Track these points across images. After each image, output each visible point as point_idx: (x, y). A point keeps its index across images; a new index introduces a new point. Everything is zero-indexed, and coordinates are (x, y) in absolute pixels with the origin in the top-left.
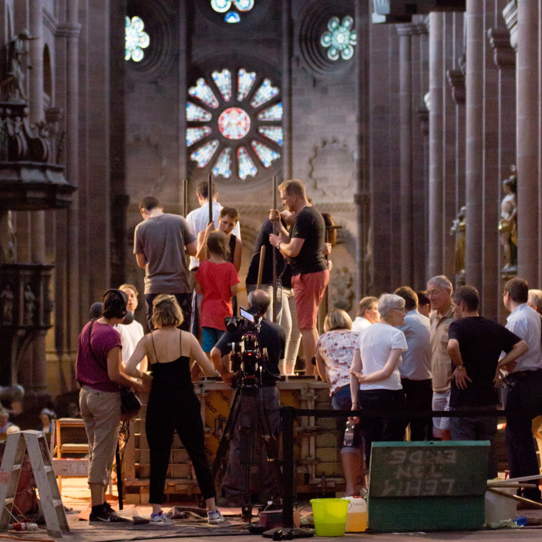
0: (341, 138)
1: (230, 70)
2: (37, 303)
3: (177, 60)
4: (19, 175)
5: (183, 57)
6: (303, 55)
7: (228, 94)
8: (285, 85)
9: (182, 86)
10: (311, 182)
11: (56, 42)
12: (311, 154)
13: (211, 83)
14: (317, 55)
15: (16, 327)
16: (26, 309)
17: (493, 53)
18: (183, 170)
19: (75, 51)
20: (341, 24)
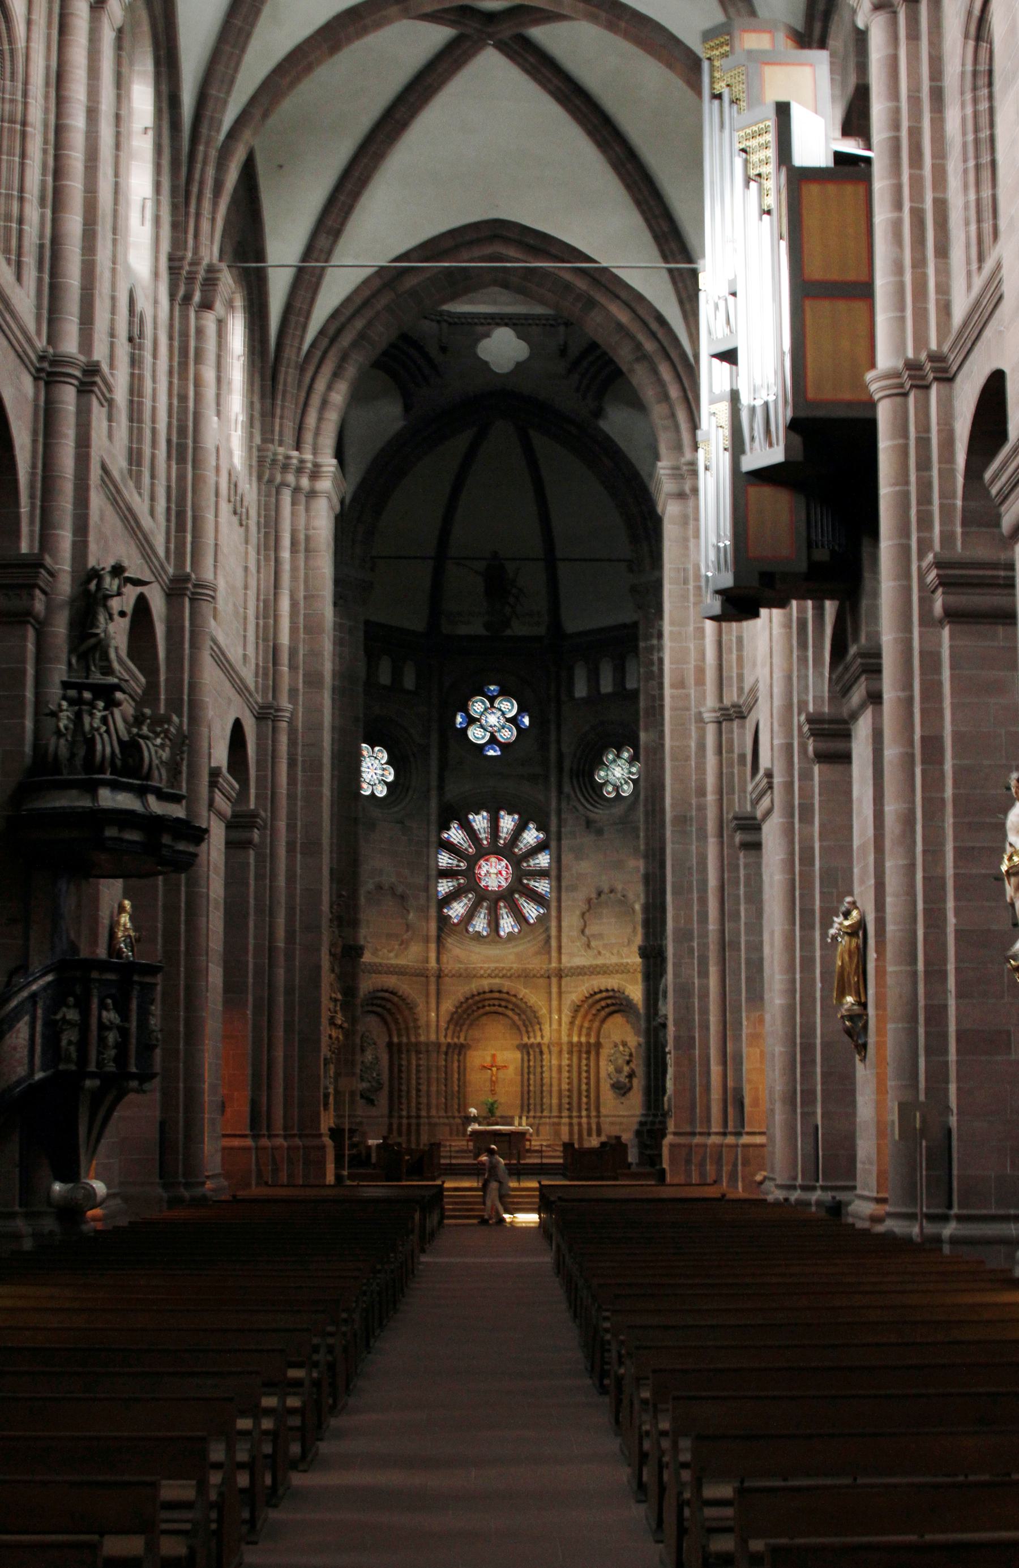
0: (619, 887)
1: (488, 812)
2: (124, 1032)
4: (95, 797)
5: (434, 793)
6: (575, 792)
7: (486, 838)
8: (553, 828)
9: (434, 828)
10: (584, 939)
11: (258, 726)
13: (467, 827)
14: (591, 792)
15: (82, 1074)
16: (102, 1040)
17: (932, 602)
18: (433, 926)
19: (284, 739)
20: (618, 756)
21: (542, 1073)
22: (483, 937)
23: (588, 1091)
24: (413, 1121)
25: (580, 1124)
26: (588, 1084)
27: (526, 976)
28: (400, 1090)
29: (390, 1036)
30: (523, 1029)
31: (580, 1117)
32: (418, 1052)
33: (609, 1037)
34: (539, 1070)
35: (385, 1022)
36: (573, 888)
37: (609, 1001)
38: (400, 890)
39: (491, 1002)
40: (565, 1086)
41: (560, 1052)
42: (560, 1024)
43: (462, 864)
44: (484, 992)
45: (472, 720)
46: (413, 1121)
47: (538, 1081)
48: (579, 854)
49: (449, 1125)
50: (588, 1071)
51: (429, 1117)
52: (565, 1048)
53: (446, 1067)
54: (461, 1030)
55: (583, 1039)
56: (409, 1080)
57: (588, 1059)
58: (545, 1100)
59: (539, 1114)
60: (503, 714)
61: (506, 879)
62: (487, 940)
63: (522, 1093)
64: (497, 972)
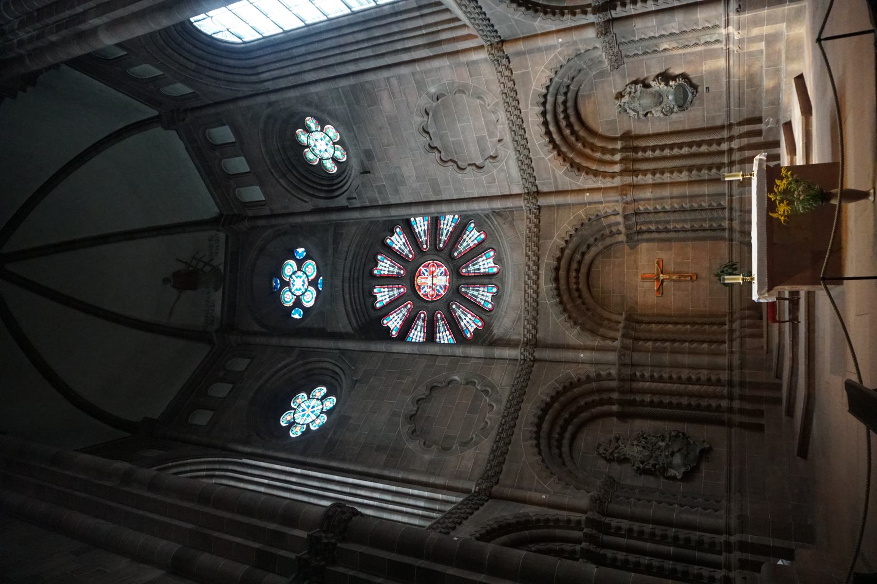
0: (418, 120)
3: (343, 351)
5: (341, 345)
12: (451, 167)
18: (475, 351)
22: (497, 292)
23: (690, 145)
24: (737, 391)
25: (741, 149)
26: (680, 146)
27: (537, 236)
28: (689, 406)
29: (610, 414)
30: (608, 241)
31: (731, 150)
32: (633, 378)
33: (613, 122)
34: (662, 217)
35: (593, 419)
36: (434, 185)
37: (563, 123)
39: (572, 280)
40: (684, 176)
41: (634, 186)
42: (599, 189)
43: (422, 315)
44: (558, 289)
45: (298, 303)
46: (737, 391)
47: (677, 216)
48: (397, 181)
49: (742, 337)
50: (662, 148)
51: (731, 368)
52: (628, 180)
53: (656, 340)
54: (609, 320)
55: (618, 157)
56: (672, 394)
57: (644, 149)
58: (705, 205)
59: (727, 213)
60: (294, 273)
61: (439, 266)
63: (694, 239)
64: (531, 273)
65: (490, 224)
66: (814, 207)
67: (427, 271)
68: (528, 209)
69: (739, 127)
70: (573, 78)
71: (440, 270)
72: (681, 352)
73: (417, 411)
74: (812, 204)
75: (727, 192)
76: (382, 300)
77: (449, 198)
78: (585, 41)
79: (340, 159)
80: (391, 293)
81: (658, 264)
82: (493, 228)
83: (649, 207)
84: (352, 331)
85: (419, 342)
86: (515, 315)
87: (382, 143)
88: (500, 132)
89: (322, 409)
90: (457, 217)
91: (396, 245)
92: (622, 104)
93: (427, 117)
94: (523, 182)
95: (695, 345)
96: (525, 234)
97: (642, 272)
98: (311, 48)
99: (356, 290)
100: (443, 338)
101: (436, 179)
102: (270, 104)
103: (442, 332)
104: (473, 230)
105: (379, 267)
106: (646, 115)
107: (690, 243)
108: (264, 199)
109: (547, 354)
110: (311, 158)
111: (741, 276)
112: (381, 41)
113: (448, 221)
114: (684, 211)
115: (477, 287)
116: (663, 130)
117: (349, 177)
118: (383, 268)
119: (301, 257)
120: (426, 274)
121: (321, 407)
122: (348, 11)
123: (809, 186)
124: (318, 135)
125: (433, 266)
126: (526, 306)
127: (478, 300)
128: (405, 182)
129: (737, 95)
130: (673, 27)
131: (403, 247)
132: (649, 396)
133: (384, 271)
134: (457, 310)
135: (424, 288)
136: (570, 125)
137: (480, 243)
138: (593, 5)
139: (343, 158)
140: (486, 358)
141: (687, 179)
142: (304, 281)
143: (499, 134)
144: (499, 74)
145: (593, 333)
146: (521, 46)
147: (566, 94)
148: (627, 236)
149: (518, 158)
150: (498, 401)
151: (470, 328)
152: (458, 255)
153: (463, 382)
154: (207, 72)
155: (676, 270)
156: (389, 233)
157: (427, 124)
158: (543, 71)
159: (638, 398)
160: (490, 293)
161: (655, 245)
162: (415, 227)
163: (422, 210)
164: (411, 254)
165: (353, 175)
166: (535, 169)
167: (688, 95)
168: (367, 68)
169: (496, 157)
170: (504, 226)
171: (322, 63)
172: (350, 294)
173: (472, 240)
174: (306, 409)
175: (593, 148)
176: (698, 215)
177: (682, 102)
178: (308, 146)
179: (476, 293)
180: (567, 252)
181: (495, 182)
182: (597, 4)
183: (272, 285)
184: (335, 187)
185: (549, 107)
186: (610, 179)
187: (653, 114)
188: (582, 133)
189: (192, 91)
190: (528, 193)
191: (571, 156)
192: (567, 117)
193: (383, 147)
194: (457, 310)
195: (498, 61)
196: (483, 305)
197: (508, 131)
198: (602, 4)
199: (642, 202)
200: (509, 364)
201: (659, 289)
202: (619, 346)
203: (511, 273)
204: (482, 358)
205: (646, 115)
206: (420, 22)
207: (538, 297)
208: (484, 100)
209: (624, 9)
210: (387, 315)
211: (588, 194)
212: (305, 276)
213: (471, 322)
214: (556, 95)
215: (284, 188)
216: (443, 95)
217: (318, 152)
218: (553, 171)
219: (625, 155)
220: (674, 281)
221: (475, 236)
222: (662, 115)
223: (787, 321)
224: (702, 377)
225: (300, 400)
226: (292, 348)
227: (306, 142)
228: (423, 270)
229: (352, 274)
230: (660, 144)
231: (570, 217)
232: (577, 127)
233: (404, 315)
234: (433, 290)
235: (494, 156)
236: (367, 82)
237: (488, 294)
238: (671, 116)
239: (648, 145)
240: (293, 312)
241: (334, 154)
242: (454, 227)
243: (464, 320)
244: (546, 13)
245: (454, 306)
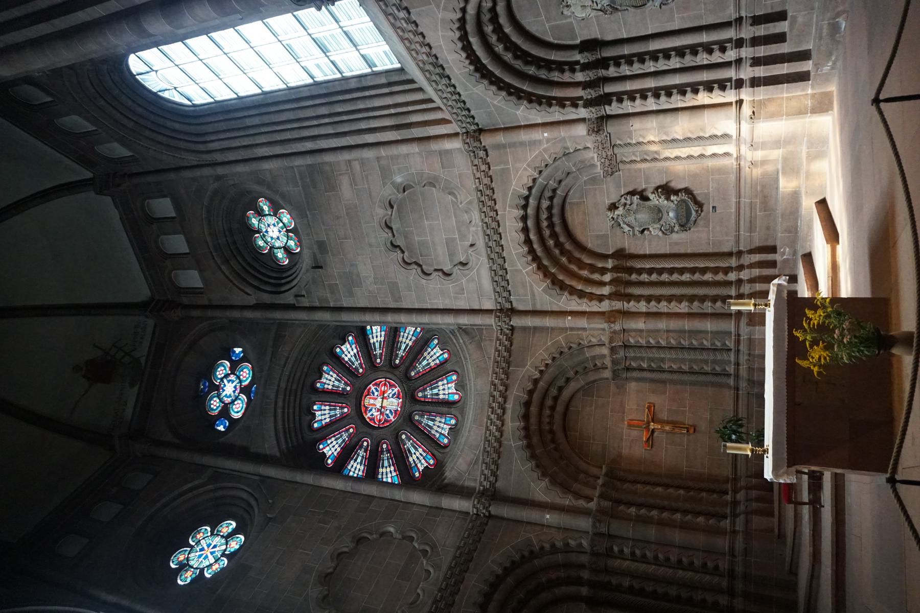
0: (380, 212)
3: (264, 479)
12: (414, 271)
18: (418, 497)
21: (660, 348)
22: (456, 425)
23: (693, 271)
25: (752, 281)
26: (682, 271)
29: (575, 598)
30: (592, 377)
33: (605, 236)
36: (394, 289)
37: (547, 233)
38: (346, 545)
40: (684, 307)
43: (365, 444)
44: (526, 428)
47: (673, 355)
48: (352, 281)
50: (660, 271)
51: (732, 551)
52: (618, 305)
55: (607, 278)
57: (640, 271)
60: (227, 376)
61: (391, 386)
62: (460, 418)
63: (693, 384)
65: (455, 341)
66: (866, 356)
67: (377, 391)
68: (499, 328)
69: (749, 256)
70: (560, 181)
71: (393, 390)
72: (672, 525)
73: (335, 569)
74: (862, 351)
75: (733, 330)
76: (321, 420)
77: (410, 307)
78: (574, 139)
79: (293, 250)
80: (332, 413)
81: (649, 408)
82: (458, 348)
83: (641, 341)
84: (278, 454)
85: (357, 477)
86: (472, 455)
87: (338, 235)
88: (473, 236)
89: (225, 550)
90: (419, 330)
91: (346, 356)
92: (615, 217)
93: (391, 210)
94: (495, 296)
95: (689, 517)
96: (492, 358)
97: (630, 418)
98: (266, 119)
99: (292, 405)
100: (387, 474)
101: (396, 283)
102: (218, 178)
103: (386, 467)
104: (435, 347)
105: (324, 380)
106: (642, 232)
107: (688, 388)
108: (202, 286)
109: (505, 511)
110: (261, 245)
111: (750, 446)
112: (345, 118)
113: (408, 334)
114: (683, 348)
115: (433, 416)
116: (662, 251)
117: (300, 272)
118: (328, 382)
119: (237, 359)
120: (376, 394)
121: (224, 547)
122: (311, 81)
123: (859, 323)
124: (271, 220)
125: (385, 385)
126: (486, 446)
127: (433, 432)
128: (361, 283)
129: (748, 220)
130: (676, 132)
131: (353, 359)
132: (628, 579)
133: (329, 385)
134: (407, 442)
135: (371, 410)
136: (554, 235)
137: (442, 364)
138: (585, 98)
139: (297, 249)
140: (431, 507)
141: (686, 310)
142: (235, 387)
143: (471, 238)
144: (474, 168)
145: (566, 488)
146: (500, 138)
147: (551, 199)
148: (614, 372)
149: (491, 267)
150: (437, 567)
151: (419, 465)
152: (415, 374)
153: (399, 536)
154: (147, 133)
155: (670, 419)
156: (340, 342)
157: (390, 219)
158: (525, 169)
159: (614, 581)
160: (447, 424)
161: (647, 385)
162: (370, 336)
163: (377, 317)
164: (362, 367)
165: (303, 269)
166: (510, 283)
167: (691, 214)
168: (326, 147)
169: (466, 264)
170: (469, 346)
171: (277, 137)
172: (283, 408)
173: (433, 358)
174: (206, 548)
175: (581, 265)
176: (699, 356)
177: (684, 220)
178: (259, 231)
179: (431, 423)
180: (541, 384)
181: (464, 294)
182: (589, 97)
183: (199, 386)
184: (283, 281)
185: (530, 211)
186: (597, 303)
187: (651, 232)
188: (568, 246)
189: (130, 154)
190: (501, 310)
191: (553, 271)
192: (551, 226)
193: (339, 239)
194: (407, 442)
195: (474, 152)
196: (438, 439)
197: (481, 234)
198: (596, 98)
199: (633, 334)
200: (458, 518)
201: (648, 439)
202: (594, 509)
203: (473, 403)
204: (428, 506)
205: (642, 232)
206: (389, 101)
207: (502, 436)
208: (456, 198)
209: (619, 105)
210: (324, 439)
211: (570, 318)
212: (238, 381)
213: (421, 458)
214: (540, 199)
215: (224, 274)
216: (411, 187)
217: (269, 239)
218: (531, 286)
219: (615, 275)
220: (667, 433)
221: (438, 355)
222: (660, 234)
223: (805, 504)
224: (695, 561)
225: (201, 534)
226: (205, 467)
227: (256, 226)
228: (373, 388)
229: (290, 384)
230: (658, 266)
231: (546, 343)
232: (562, 239)
233: (344, 441)
234: (382, 413)
235: (464, 262)
236: (326, 163)
237: (445, 426)
238: (671, 235)
239: (643, 266)
240: (217, 422)
241: (286, 243)
242: (414, 341)
243: (414, 456)
244: (530, 101)
245: (404, 437)
